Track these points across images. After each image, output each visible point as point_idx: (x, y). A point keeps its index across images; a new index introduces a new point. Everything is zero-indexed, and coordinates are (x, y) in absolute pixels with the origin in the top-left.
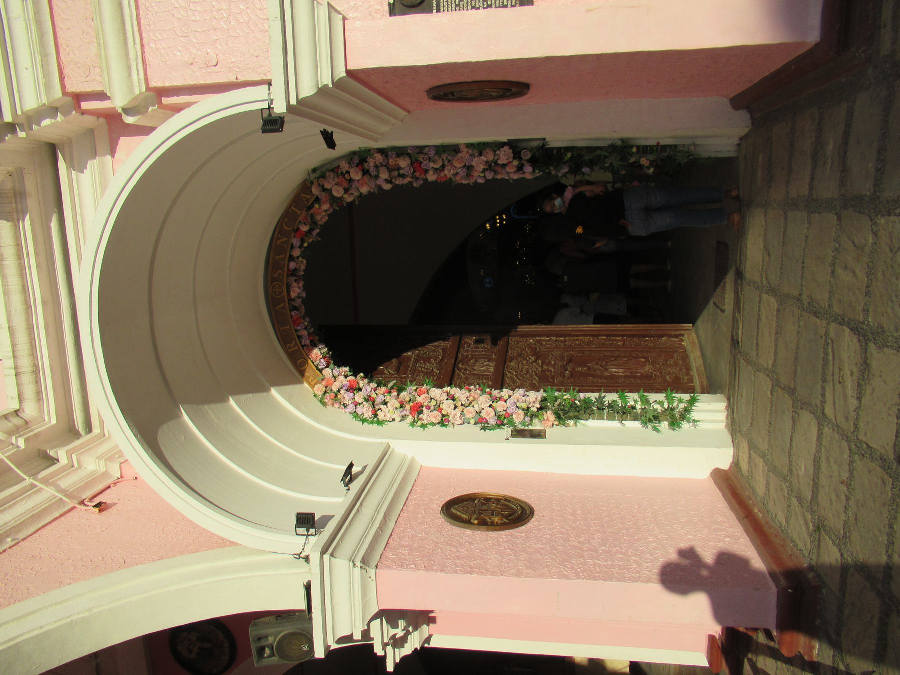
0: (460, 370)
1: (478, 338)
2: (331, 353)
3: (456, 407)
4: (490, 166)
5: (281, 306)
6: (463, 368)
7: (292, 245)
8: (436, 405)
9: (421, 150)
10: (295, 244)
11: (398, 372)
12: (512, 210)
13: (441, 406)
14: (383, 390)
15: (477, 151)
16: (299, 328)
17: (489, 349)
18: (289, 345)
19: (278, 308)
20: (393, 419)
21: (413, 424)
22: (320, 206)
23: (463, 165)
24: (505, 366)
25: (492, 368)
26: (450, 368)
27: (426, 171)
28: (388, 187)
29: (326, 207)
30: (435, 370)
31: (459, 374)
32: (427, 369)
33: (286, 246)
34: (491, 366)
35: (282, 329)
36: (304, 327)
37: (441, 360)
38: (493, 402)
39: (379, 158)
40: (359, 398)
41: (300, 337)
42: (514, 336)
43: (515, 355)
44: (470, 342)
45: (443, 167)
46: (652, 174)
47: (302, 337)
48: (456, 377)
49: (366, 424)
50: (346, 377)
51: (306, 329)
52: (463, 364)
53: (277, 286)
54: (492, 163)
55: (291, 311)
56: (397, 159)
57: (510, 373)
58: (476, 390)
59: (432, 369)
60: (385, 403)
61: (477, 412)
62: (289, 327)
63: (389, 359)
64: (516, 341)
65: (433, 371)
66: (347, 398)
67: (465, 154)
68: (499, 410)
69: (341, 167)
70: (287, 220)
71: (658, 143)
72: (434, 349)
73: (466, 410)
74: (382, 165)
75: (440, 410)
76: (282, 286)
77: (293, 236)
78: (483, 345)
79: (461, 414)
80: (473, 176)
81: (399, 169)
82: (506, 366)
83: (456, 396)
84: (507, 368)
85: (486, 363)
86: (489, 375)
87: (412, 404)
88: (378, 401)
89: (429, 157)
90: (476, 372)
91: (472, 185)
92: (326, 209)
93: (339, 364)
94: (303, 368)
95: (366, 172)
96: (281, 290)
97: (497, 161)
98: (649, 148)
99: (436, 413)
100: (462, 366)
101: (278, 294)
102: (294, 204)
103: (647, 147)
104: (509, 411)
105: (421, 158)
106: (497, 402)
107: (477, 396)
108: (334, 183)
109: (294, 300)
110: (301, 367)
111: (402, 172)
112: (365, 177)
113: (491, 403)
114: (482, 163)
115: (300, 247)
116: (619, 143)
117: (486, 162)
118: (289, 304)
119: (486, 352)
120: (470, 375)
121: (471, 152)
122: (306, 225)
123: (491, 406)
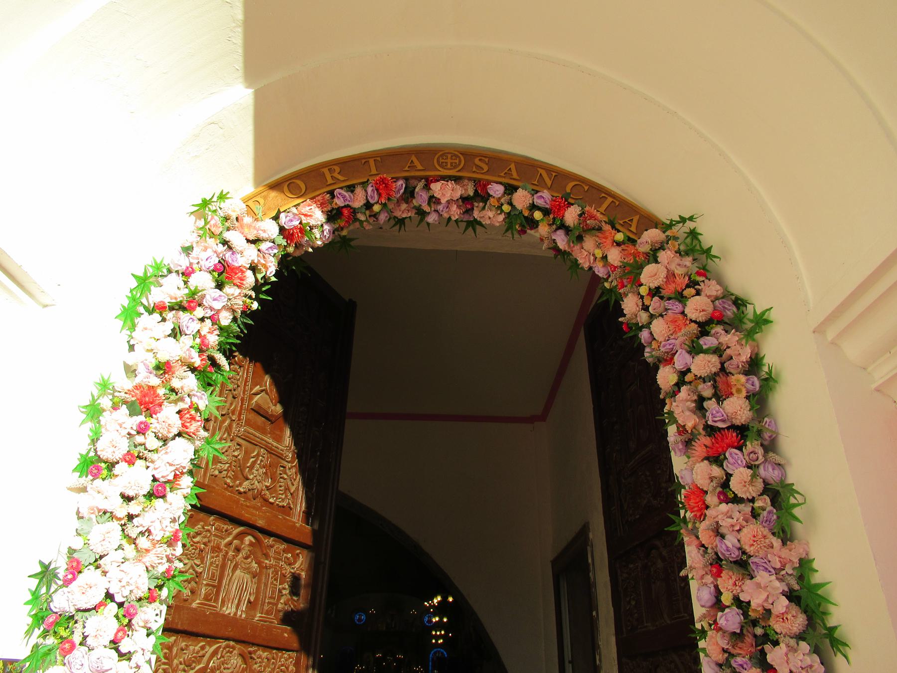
0: (241, 536)
1: (303, 582)
2: (310, 250)
3: (127, 499)
4: (755, 623)
5: (417, 163)
6: (242, 542)
7: (537, 192)
8: (146, 449)
9: (770, 446)
10: (539, 194)
11: (252, 409)
12: (439, 649)
13: (139, 462)
14: (213, 339)
15: (796, 587)
16: (370, 189)
17: (276, 604)
18: (337, 169)
19: (414, 158)
20: (133, 345)
21: (105, 386)
22: (619, 244)
23: (750, 550)
24: (234, 640)
25: (234, 610)
26: (246, 516)
27: (716, 459)
28: (666, 377)
29: (615, 256)
30: (246, 484)
31: (230, 534)
32: (252, 467)
33: (536, 183)
34: (237, 608)
35: (372, 162)
36: (372, 201)
37: (266, 500)
38: (120, 605)
39: (745, 354)
40: (203, 281)
41: (351, 188)
42: (297, 664)
43: (256, 666)
44: (297, 565)
45: (737, 500)
47: (352, 191)
48: (226, 527)
49: (134, 283)
50: (254, 268)
51: (368, 206)
52: (251, 544)
53: (457, 161)
54: (763, 627)
55: (406, 179)
56: (744, 394)
57: (215, 653)
58: (169, 560)
59: (251, 477)
60: (176, 333)
61: (101, 557)
62: (374, 171)
63: (283, 400)
64: (287, 668)
65: (247, 479)
66: (204, 255)
67: (777, 553)
69: (706, 281)
70: (586, 188)
72: (292, 491)
73: (115, 526)
74: (722, 364)
75: (130, 459)
76: (458, 169)
77: (556, 195)
78: (288, 592)
80: (718, 575)
81: (719, 397)
82: (232, 643)
83: (158, 503)
84: (228, 646)
85: (246, 597)
86: (216, 600)
87: (161, 391)
88: (184, 317)
89: (758, 466)
90: (228, 571)
91: (682, 573)
92: (609, 258)
93: (284, 262)
94: (286, 188)
95: (704, 328)
96: (449, 166)
97: (776, 643)
99: (124, 446)
100: (247, 543)
101: (441, 160)
102: (617, 203)
104: (80, 651)
105: (752, 445)
106: (117, 617)
107: (150, 559)
108: (673, 267)
109: (427, 187)
110: (288, 186)
111: (710, 405)
113: (119, 599)
114: (770, 601)
115: (533, 207)
117: (768, 612)
118: (419, 179)
119: (271, 598)
120: (225, 556)
122: (580, 215)
123: (109, 596)
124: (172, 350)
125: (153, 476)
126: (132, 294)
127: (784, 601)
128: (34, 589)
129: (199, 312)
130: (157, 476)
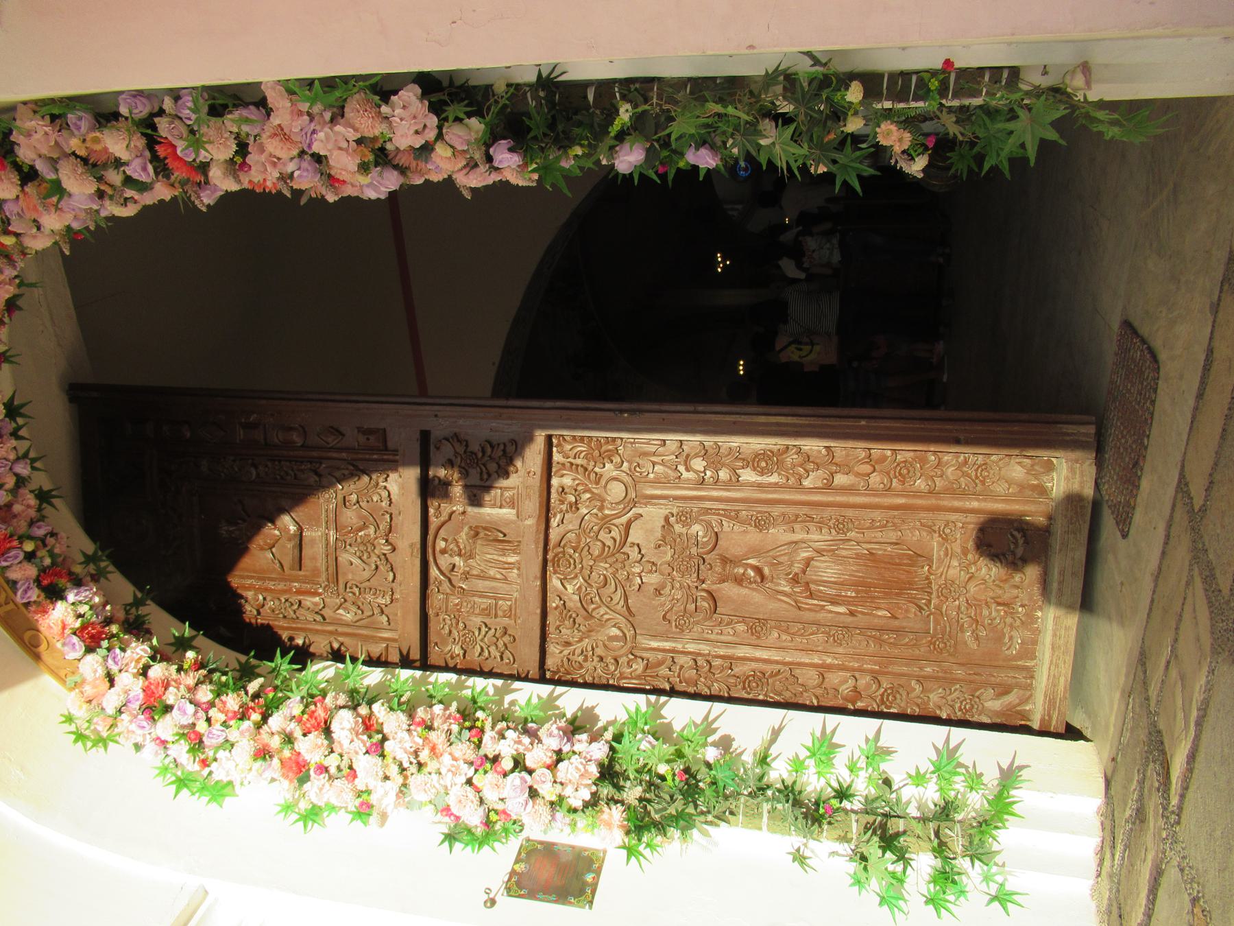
14: (232, 701)
21: (288, 808)
36: (22, 556)
40: (166, 727)
46: (920, 176)
49: (185, 792)
68: (491, 796)
71: (948, 63)
79: (401, 791)
98: (914, 78)
103: (906, 75)
112: (27, 189)
113: (471, 772)
114: (345, 145)
116: (805, 68)
117: (359, 142)
121: (305, 107)
123: (469, 782)
124: (245, 747)
125: (364, 754)
126: (196, 792)
127: (338, 128)
128: (463, 845)
129: (202, 727)
130: (364, 751)
